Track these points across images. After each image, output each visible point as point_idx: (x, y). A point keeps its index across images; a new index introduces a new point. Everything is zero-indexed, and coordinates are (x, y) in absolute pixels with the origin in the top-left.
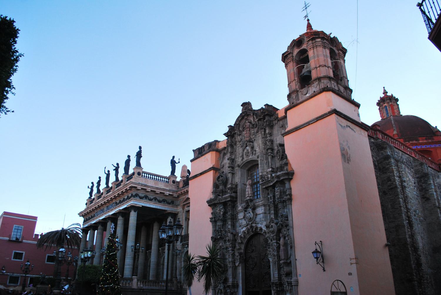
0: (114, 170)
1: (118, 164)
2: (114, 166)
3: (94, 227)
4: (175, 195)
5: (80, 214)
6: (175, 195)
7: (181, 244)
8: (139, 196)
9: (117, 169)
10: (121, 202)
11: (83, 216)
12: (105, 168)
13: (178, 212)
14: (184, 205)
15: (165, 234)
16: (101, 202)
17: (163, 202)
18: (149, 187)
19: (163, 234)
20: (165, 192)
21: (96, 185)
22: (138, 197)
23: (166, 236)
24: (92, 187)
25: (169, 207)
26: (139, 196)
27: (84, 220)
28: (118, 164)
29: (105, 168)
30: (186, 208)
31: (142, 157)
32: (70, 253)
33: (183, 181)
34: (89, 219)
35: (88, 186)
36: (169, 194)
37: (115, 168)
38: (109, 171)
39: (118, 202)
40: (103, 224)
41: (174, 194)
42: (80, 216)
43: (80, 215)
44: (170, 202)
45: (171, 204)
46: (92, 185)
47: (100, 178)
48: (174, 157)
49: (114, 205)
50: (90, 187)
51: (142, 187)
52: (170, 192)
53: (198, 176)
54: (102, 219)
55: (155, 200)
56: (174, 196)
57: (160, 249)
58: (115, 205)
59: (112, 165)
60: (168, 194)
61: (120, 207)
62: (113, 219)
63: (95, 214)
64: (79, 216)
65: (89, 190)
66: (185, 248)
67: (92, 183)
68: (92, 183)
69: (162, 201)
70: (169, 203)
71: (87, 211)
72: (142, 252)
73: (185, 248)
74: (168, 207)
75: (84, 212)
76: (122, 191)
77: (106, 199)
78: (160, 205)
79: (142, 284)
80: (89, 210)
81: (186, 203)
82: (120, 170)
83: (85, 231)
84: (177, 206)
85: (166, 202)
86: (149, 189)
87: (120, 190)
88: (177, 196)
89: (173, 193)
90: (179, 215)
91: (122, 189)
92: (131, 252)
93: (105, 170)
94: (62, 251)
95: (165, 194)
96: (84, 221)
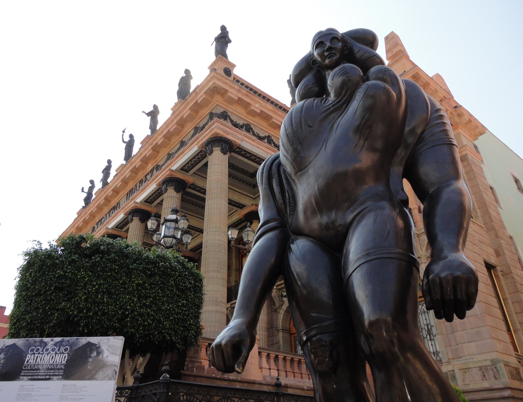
1: (155, 107)
8: (232, 121)
9: (153, 114)
12: (124, 132)
24: (91, 188)
26: (232, 121)
28: (155, 107)
29: (124, 132)
31: (230, 41)
35: (83, 189)
38: (131, 136)
46: (91, 185)
47: (109, 162)
50: (86, 190)
51: (240, 96)
59: (143, 112)
65: (86, 195)
67: (92, 182)
68: (92, 182)
79: (273, 365)
86: (257, 105)
93: (123, 135)
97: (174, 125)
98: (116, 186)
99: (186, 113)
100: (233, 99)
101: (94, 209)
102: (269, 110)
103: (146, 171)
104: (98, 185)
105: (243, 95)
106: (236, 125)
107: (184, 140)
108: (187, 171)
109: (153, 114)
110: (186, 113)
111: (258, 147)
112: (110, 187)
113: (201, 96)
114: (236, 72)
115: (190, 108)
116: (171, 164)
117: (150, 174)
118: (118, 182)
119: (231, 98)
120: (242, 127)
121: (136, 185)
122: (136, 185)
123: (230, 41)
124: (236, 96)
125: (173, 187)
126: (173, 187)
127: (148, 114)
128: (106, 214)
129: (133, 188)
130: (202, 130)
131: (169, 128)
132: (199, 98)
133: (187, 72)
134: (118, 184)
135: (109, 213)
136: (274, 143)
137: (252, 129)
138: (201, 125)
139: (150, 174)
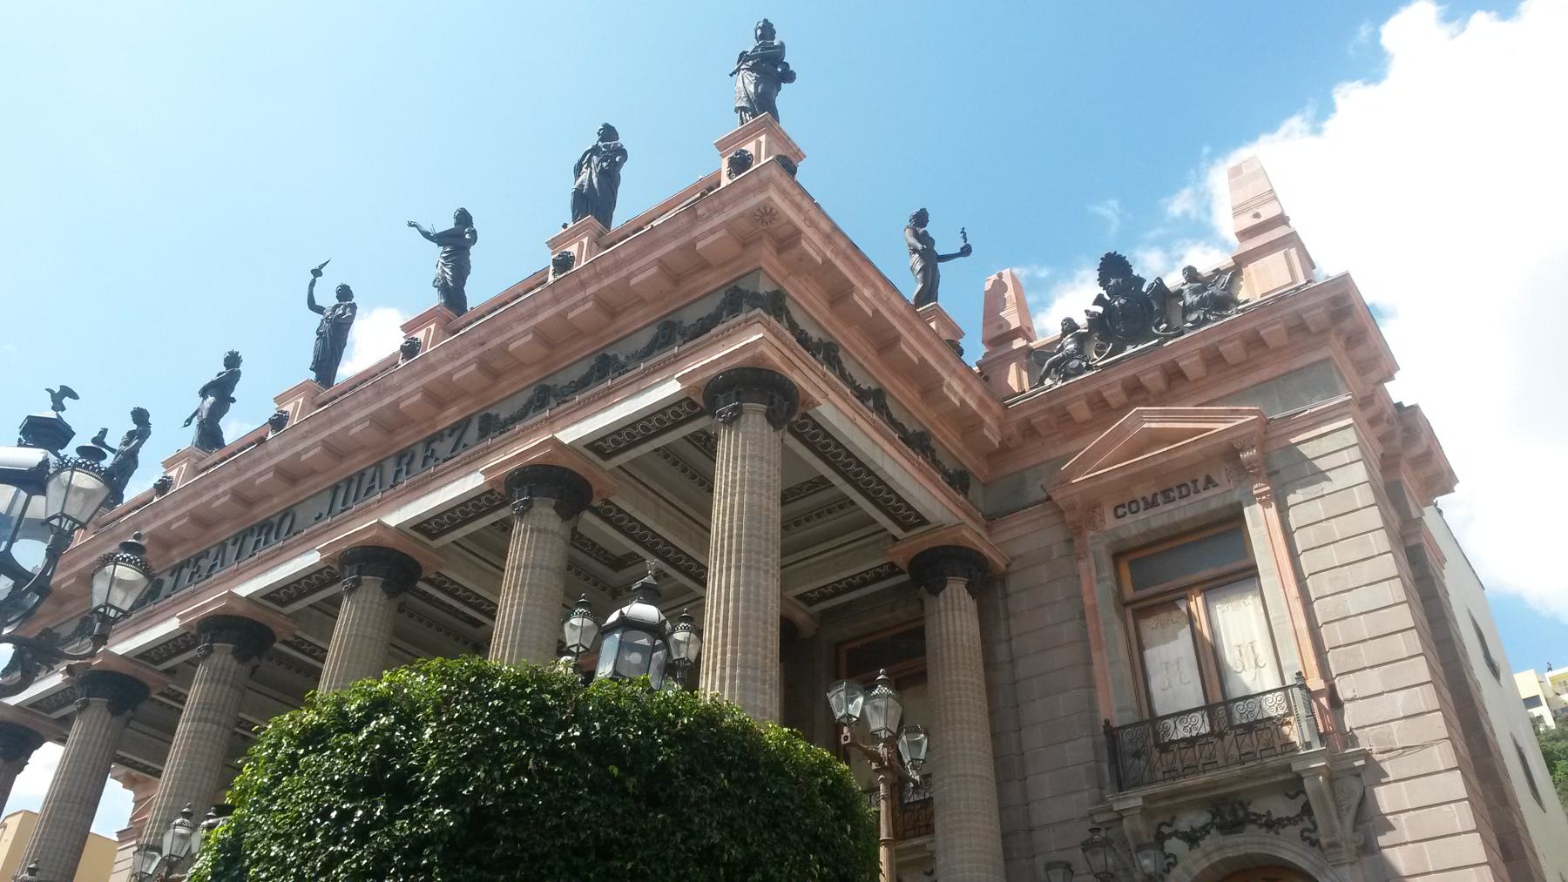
1: (464, 218)
4: (990, 429)
12: (317, 273)
18: (867, 282)
25: (952, 506)
28: (464, 218)
29: (317, 273)
30: (1110, 522)
38: (344, 293)
47: (233, 361)
48: (921, 219)
59: (411, 225)
66: (1174, 845)
67: (140, 416)
68: (140, 416)
74: (944, 499)
82: (477, 255)
86: (867, 293)
90: (1013, 584)
93: (312, 284)
97: (584, 300)
98: (299, 454)
99: (642, 270)
100: (811, 259)
101: (178, 519)
102: (894, 313)
104: (173, 434)
105: (837, 255)
106: (803, 339)
107: (610, 353)
108: (606, 456)
109: (457, 242)
110: (642, 270)
111: (853, 421)
112: (270, 455)
113: (712, 231)
114: (805, 174)
115: (659, 260)
116: (550, 421)
117: (450, 442)
118: (309, 442)
119: (804, 256)
121: (379, 465)
122: (379, 465)
123: (789, 76)
124: (819, 252)
125: (553, 502)
126: (553, 502)
127: (440, 239)
128: (223, 545)
129: (362, 474)
131: (563, 305)
132: (704, 236)
133: (608, 133)
134: (306, 450)
135: (241, 538)
136: (889, 415)
137: (840, 362)
138: (690, 318)
139: (450, 442)
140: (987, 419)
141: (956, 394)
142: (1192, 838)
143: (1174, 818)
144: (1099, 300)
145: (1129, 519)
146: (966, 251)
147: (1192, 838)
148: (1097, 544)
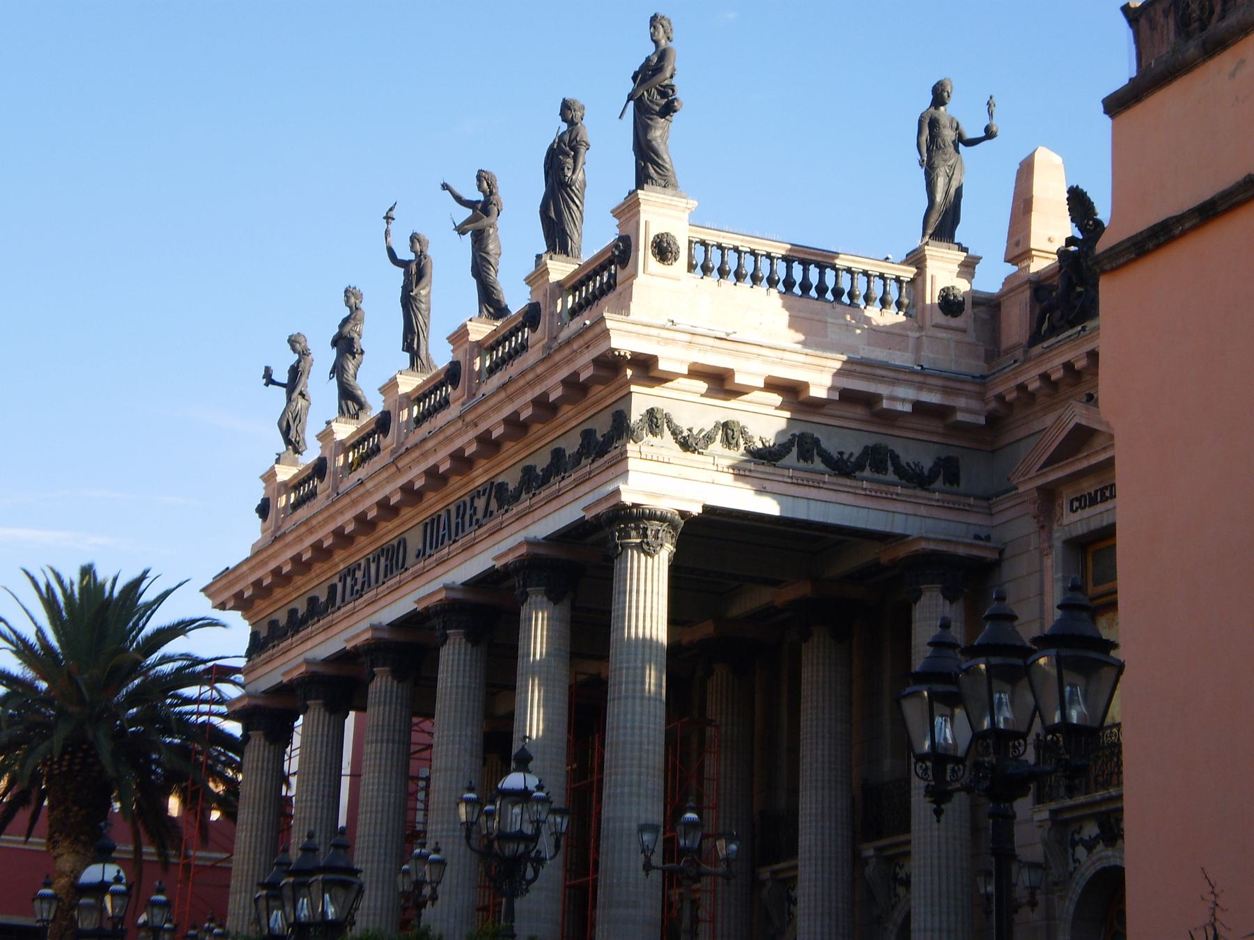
0: (461, 230)
2: (459, 199)
3: (337, 686)
4: (967, 410)
5: (219, 592)
6: (968, 410)
7: (1045, 815)
10: (532, 480)
11: (242, 604)
12: (388, 218)
13: (1001, 552)
14: (1049, 494)
15: (959, 712)
16: (377, 487)
17: (867, 473)
19: (938, 720)
20: (883, 390)
21: (323, 356)
22: (667, 432)
23: (966, 735)
24: (295, 373)
27: (254, 636)
30: (1069, 518)
32: (162, 898)
33: (1028, 293)
34: (296, 623)
36: (918, 406)
37: (468, 212)
39: (512, 480)
40: (406, 652)
41: (961, 402)
42: (222, 606)
43: (220, 600)
44: (927, 464)
45: (939, 484)
48: (939, 96)
49: (480, 503)
50: (282, 376)
52: (921, 387)
53: (1183, 234)
54: (391, 624)
55: (805, 455)
56: (960, 417)
57: (869, 851)
58: (494, 505)
59: (445, 187)
60: (908, 408)
61: (528, 520)
62: (486, 614)
63: (333, 589)
64: (209, 602)
66: (1081, 852)
69: (860, 466)
70: (916, 479)
71: (273, 565)
72: (727, 877)
73: (1074, 844)
74: (909, 509)
75: (253, 570)
76: (537, 391)
77: (416, 461)
78: (844, 498)
80: (290, 553)
81: (1068, 471)
83: (269, 717)
84: (988, 500)
85: (891, 469)
87: (521, 391)
88: (982, 421)
89: (946, 391)
91: (539, 379)
92: (642, 874)
93: (387, 233)
94: (101, 888)
95: (885, 404)
96: (257, 646)
103: (472, 480)
120: (709, 439)
130: (601, 454)
140: (961, 402)
141: (903, 400)
142: (1090, 846)
143: (1081, 828)
144: (1070, 241)
145: (1080, 514)
146: (989, 134)
147: (1090, 846)
148: (1059, 535)
